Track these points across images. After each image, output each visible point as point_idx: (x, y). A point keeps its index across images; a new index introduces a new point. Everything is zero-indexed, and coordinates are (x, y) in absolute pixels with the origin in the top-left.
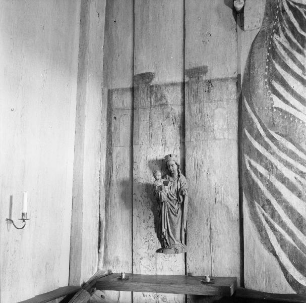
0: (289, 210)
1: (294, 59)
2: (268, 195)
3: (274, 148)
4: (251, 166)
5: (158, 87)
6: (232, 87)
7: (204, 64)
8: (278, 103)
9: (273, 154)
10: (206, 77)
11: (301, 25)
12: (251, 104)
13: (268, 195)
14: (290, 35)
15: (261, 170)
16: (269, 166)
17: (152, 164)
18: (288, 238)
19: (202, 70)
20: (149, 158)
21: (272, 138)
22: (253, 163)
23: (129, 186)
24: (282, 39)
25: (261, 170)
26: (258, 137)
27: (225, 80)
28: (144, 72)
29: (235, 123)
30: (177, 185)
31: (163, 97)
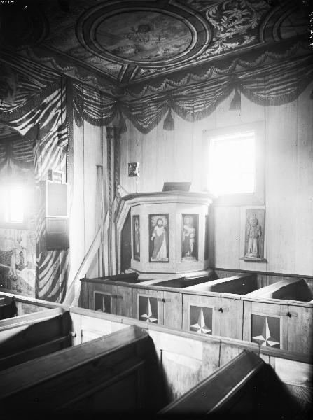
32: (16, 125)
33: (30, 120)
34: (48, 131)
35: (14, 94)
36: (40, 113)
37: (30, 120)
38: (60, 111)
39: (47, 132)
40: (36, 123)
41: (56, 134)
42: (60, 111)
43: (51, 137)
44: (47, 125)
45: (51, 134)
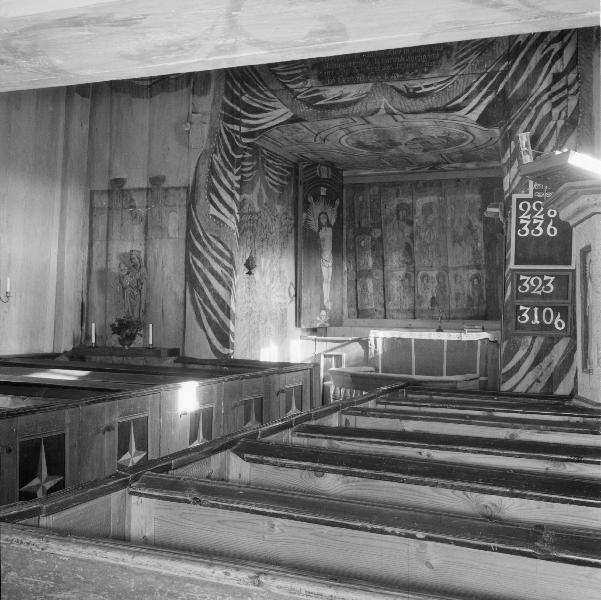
0: (216, 295)
1: (226, 175)
2: (203, 285)
3: (209, 248)
4: (194, 262)
5: (128, 190)
6: (183, 195)
7: (163, 173)
8: (216, 213)
9: (208, 251)
10: (165, 185)
11: (233, 149)
12: (195, 211)
13: (203, 285)
14: (225, 155)
15: (200, 264)
16: (205, 261)
17: (122, 257)
18: (214, 318)
19: (163, 179)
20: (120, 251)
21: (207, 238)
22: (195, 258)
23: (104, 273)
24: (218, 158)
25: (200, 264)
26: (198, 238)
27: (178, 189)
28: (118, 177)
29: (184, 225)
30: (138, 276)
31: (132, 200)
32: (458, 108)
33: (485, 90)
34: (527, 95)
35: (454, 54)
36: (509, 68)
37: (485, 90)
38: (557, 47)
39: (523, 100)
40: (500, 88)
41: (545, 97)
42: (557, 47)
43: (532, 105)
44: (523, 85)
45: (532, 99)
